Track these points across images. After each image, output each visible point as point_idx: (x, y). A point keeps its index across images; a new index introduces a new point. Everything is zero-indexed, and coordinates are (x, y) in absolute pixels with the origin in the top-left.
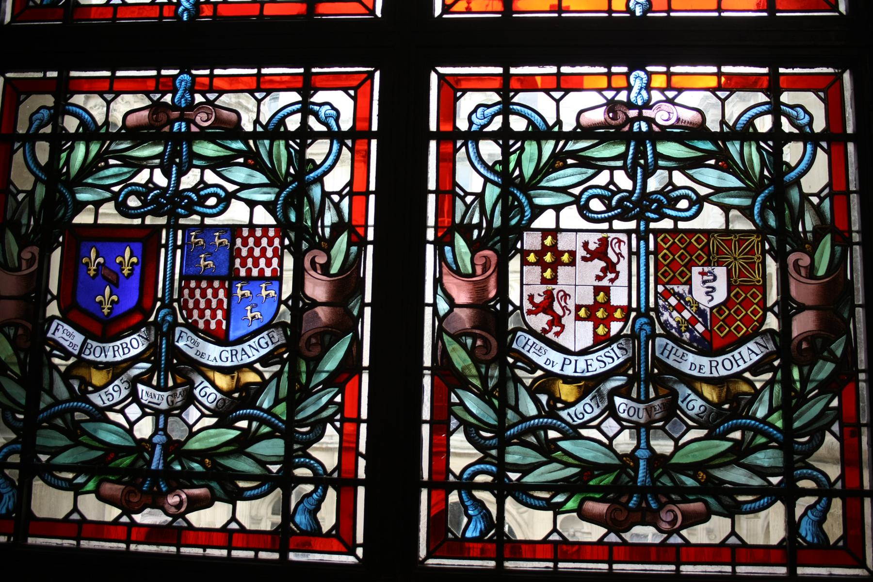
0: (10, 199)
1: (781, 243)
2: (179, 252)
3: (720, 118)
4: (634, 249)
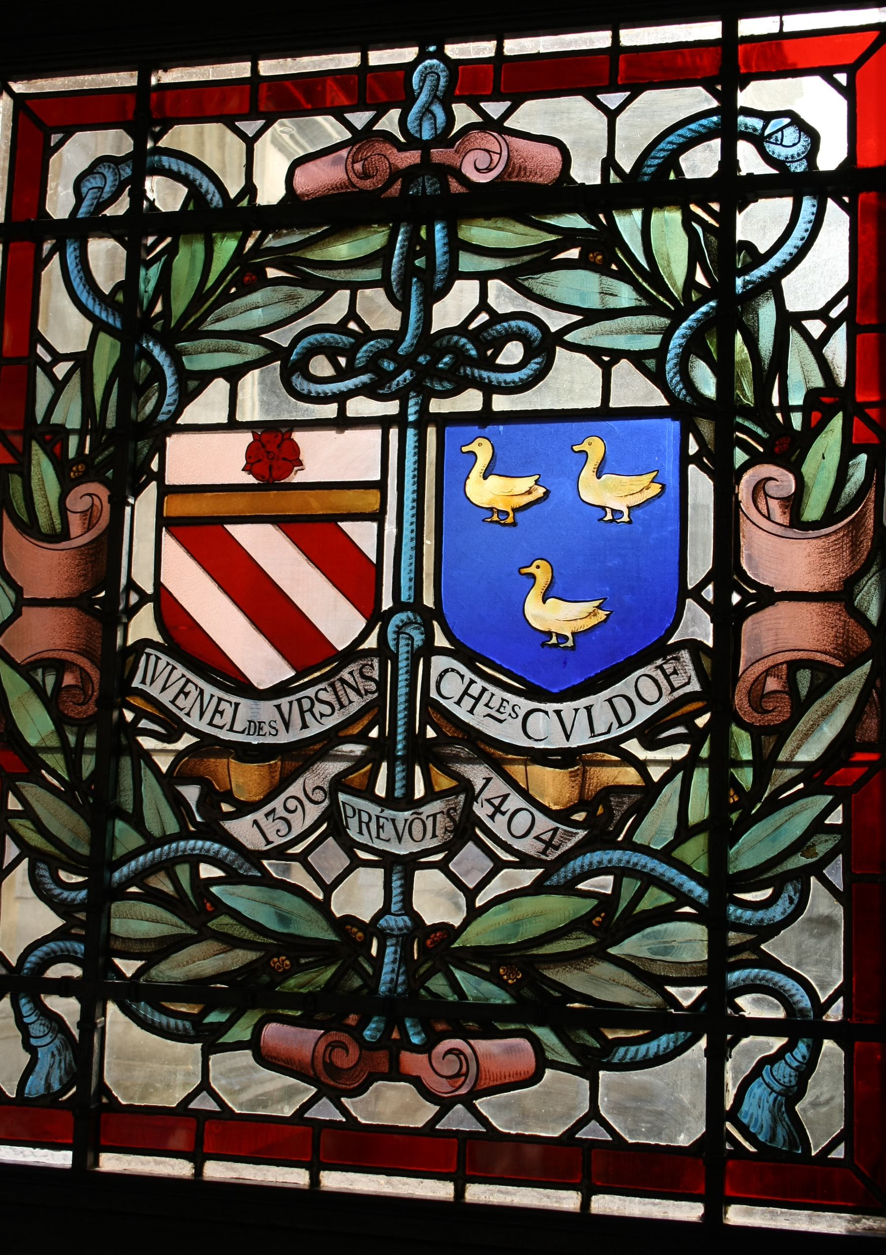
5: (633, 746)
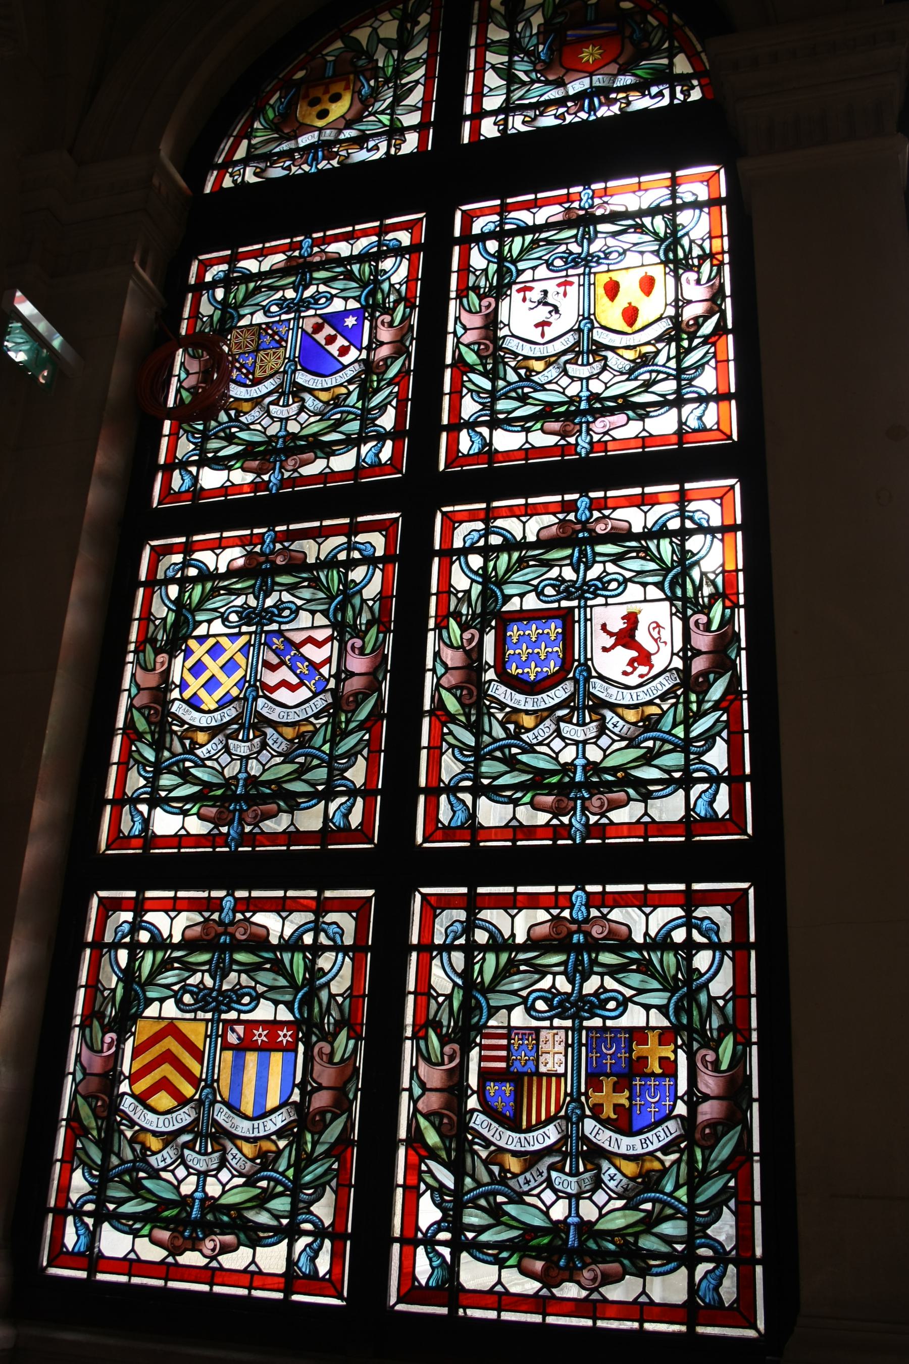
0: (99, 994)
1: (691, 1039)
2: (220, 1039)
3: (644, 930)
4: (570, 1042)
5: (312, 720)
